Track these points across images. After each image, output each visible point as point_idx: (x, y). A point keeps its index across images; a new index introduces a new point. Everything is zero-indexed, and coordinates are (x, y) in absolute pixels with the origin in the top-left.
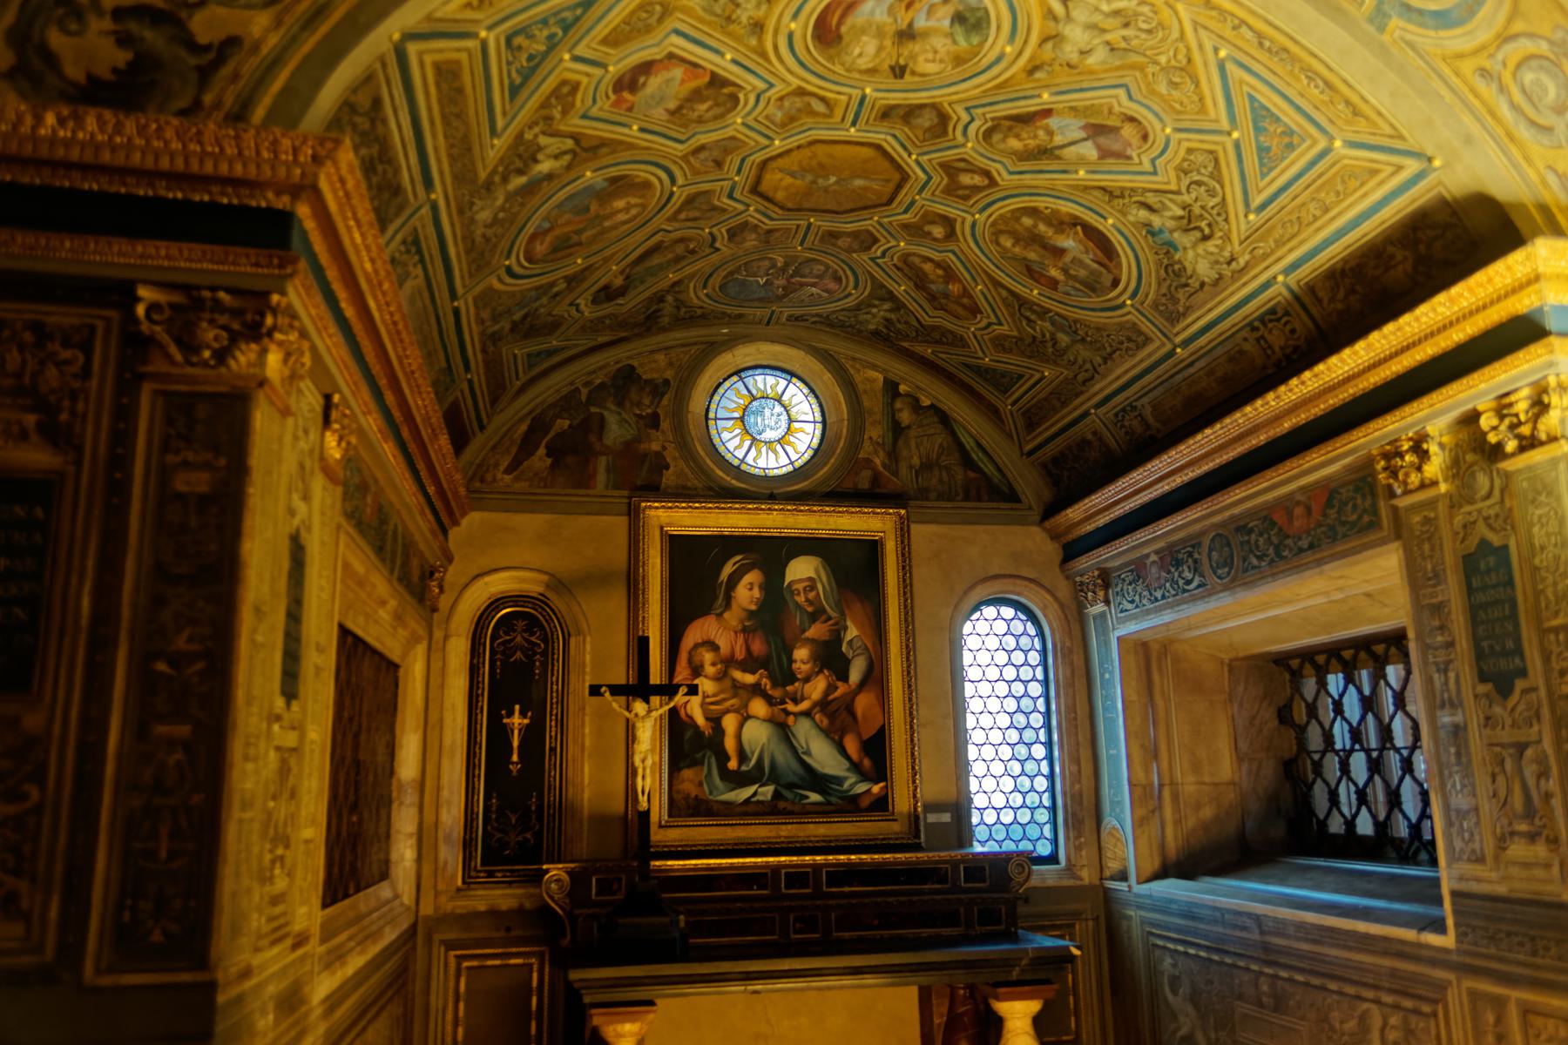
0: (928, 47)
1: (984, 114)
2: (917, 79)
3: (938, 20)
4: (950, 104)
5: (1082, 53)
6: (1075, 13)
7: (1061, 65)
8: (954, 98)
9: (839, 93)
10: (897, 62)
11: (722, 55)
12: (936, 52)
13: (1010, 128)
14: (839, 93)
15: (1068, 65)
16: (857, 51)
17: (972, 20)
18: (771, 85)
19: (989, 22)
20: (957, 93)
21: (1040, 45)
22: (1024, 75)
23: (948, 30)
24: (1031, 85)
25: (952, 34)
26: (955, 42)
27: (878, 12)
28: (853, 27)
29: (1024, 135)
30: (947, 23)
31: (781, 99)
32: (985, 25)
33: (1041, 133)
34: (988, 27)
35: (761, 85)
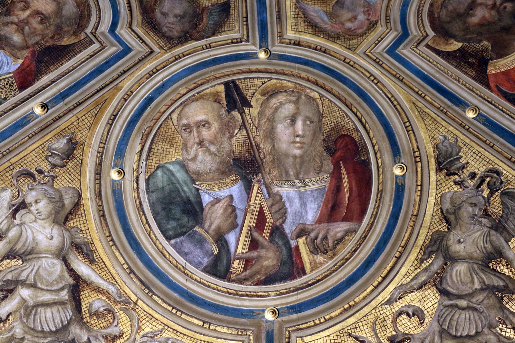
0: (213, 148)
1: (103, 47)
2: (208, 89)
3: (218, 200)
4: (152, 52)
5: (23, 205)
6: (58, 267)
7: (40, 172)
8: (149, 66)
9: (298, 44)
10: (242, 113)
11: (481, 117)
12: (201, 143)
13: (59, 31)
14: (298, 44)
15: (31, 175)
16: (299, 124)
17: (177, 211)
18: (392, 51)
19: (155, 215)
20: (151, 74)
21: (80, 197)
22: (79, 137)
23: (202, 186)
24: (63, 124)
25: (193, 181)
26: (183, 166)
27: (297, 202)
28: (319, 171)
29: (35, 23)
30: (206, 199)
31: (373, 25)
32: (159, 208)
33: (17, 38)
34: (152, 206)
35: (405, 51)
